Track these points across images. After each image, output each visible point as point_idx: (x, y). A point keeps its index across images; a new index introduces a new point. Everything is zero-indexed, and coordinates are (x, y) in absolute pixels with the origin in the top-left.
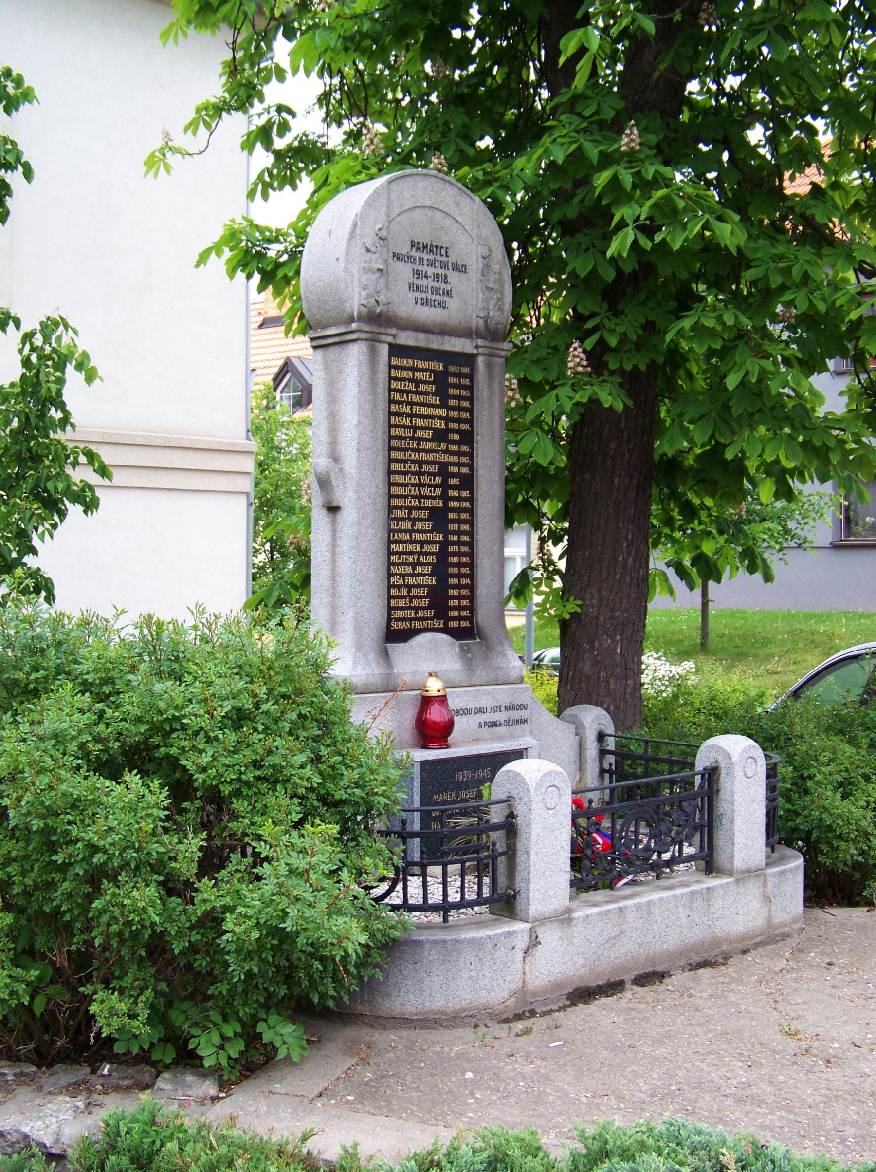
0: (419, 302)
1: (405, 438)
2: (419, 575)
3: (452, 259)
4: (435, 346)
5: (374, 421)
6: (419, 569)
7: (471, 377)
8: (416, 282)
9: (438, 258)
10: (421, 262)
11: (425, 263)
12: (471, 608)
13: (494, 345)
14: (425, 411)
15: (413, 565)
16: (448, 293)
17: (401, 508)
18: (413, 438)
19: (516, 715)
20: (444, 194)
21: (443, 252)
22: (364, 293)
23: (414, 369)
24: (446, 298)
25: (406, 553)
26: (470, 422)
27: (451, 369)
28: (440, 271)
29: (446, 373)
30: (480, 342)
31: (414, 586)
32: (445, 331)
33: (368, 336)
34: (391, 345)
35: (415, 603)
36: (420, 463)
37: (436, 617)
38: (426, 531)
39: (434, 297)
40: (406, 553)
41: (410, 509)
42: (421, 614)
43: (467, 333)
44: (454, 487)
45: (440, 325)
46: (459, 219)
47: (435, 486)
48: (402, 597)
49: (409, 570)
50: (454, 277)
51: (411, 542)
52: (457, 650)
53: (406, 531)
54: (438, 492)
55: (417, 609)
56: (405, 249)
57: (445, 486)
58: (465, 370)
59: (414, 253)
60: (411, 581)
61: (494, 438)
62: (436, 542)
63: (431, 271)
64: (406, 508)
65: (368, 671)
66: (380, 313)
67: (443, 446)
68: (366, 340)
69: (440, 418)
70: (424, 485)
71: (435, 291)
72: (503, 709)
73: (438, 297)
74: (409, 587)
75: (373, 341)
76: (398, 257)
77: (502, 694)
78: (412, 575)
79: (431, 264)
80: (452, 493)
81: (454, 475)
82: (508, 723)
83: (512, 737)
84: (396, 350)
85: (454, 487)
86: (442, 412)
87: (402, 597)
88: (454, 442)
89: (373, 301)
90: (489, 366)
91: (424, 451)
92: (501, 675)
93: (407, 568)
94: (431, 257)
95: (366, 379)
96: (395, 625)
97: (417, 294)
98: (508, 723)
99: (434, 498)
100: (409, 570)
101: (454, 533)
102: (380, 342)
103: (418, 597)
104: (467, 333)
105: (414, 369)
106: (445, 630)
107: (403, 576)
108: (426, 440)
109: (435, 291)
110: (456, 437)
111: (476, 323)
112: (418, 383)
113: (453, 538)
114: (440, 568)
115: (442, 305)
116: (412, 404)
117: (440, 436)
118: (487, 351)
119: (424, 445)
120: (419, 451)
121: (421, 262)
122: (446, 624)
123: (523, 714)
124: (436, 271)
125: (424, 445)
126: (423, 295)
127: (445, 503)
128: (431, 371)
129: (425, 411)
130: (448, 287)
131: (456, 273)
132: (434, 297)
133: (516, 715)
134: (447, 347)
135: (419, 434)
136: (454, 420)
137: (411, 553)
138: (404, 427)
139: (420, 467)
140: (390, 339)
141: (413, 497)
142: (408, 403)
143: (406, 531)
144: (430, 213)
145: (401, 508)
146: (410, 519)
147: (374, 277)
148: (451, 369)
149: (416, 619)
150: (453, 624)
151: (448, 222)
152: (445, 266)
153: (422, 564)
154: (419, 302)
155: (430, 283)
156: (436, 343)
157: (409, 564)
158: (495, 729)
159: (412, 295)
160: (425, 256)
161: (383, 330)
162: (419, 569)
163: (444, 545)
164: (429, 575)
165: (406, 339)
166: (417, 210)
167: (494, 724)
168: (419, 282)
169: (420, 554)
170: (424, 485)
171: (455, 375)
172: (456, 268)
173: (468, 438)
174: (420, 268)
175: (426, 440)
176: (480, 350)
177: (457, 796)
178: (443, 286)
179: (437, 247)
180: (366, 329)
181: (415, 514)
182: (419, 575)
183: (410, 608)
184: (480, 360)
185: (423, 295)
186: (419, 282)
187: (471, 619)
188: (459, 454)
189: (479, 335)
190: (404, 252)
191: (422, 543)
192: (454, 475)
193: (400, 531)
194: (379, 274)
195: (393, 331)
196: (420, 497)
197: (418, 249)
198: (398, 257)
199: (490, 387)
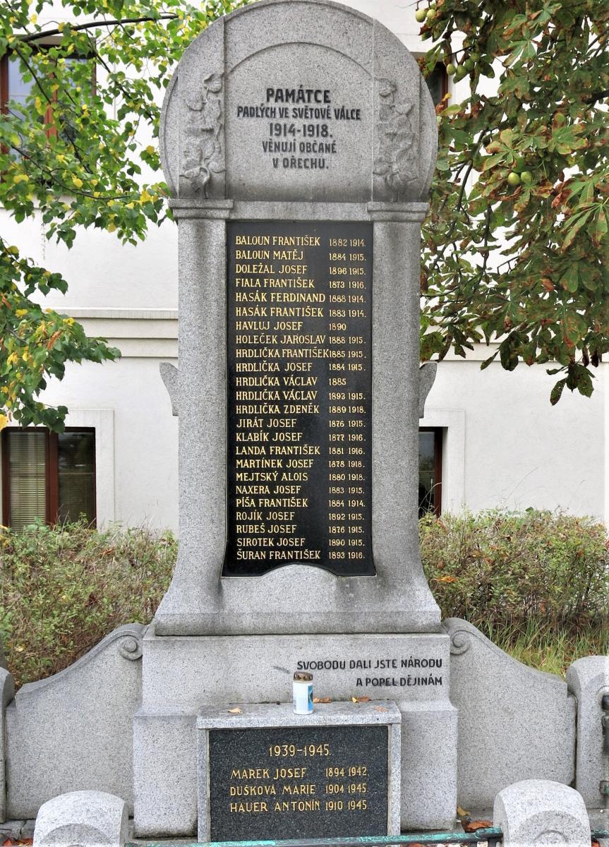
0: (280, 164)
1: (258, 333)
2: (280, 496)
3: (337, 102)
4: (300, 216)
5: (204, 315)
6: (279, 489)
7: (368, 251)
8: (275, 139)
9: (313, 105)
10: (284, 113)
11: (291, 114)
12: (367, 537)
13: (397, 206)
14: (287, 297)
15: (272, 485)
16: (330, 149)
17: (252, 417)
18: (271, 332)
19: (423, 672)
20: (321, 22)
21: (321, 97)
22: (184, 162)
23: (270, 248)
24: (325, 155)
25: (260, 470)
26: (368, 307)
27: (333, 242)
28: (315, 122)
29: (325, 249)
30: (371, 205)
31: (273, 509)
32: (323, 196)
33: (192, 213)
34: (229, 223)
35: (274, 529)
36: (283, 362)
37: (309, 545)
38: (291, 444)
39: (305, 156)
40: (260, 470)
41: (267, 417)
42: (283, 542)
43: (362, 195)
44: (338, 389)
45: (316, 189)
46: (347, 51)
47: (307, 389)
48: (253, 523)
49: (264, 490)
50: (338, 128)
51: (268, 457)
52: (334, 588)
53: (260, 444)
54: (311, 395)
55: (276, 537)
56: (258, 100)
57: (323, 388)
58: (356, 243)
59: (272, 103)
60: (267, 503)
61: (400, 326)
62: (308, 457)
63: (299, 123)
64: (259, 416)
65: (185, 609)
66: (210, 181)
67: (320, 339)
68: (190, 218)
69: (316, 304)
70: (289, 388)
71: (306, 147)
72: (398, 664)
73: (312, 155)
74: (265, 511)
75: (200, 220)
76: (246, 112)
77: (401, 647)
78: (271, 496)
79: (300, 114)
80: (333, 396)
81: (337, 374)
82: (405, 682)
83: (413, 699)
84: (233, 227)
85: (338, 389)
86: (319, 298)
87: (253, 523)
88: (337, 333)
89: (197, 169)
90: (394, 236)
91: (289, 346)
92: (401, 622)
93: (262, 488)
94: (301, 105)
95: (190, 264)
96: (241, 555)
97: (278, 155)
98: (405, 682)
99: (306, 403)
100: (264, 490)
101: (336, 444)
102: (212, 218)
103: (279, 523)
104: (362, 195)
105: (270, 248)
106: (323, 563)
107: (256, 497)
108: (292, 333)
109: (306, 147)
110: (341, 327)
111: (375, 182)
112: (279, 264)
113: (333, 451)
114: (315, 486)
115: (321, 164)
116: (268, 290)
117: (309, 327)
118: (389, 215)
119: (288, 339)
120: (280, 347)
121: (284, 113)
122: (324, 555)
123: (435, 672)
124: (307, 122)
125: (288, 339)
126: (288, 155)
127: (324, 409)
128: (299, 248)
129: (287, 297)
130: (330, 141)
131: (340, 122)
132: (305, 156)
133: (423, 672)
134: (322, 216)
135: (280, 326)
136: (337, 306)
137: (269, 470)
138: (257, 319)
139: (283, 366)
140: (225, 214)
141: (271, 402)
142: (262, 290)
143: (260, 444)
144: (300, 51)
145: (252, 417)
146: (265, 430)
147: (197, 141)
148: (333, 242)
149: (275, 548)
150: (333, 555)
151: (330, 58)
152: (324, 114)
153: (285, 483)
154: (280, 164)
155: (299, 138)
156: (303, 212)
157: (264, 483)
158: (384, 687)
159: (268, 157)
160: (290, 105)
161: (209, 204)
162: (279, 489)
163: (324, 458)
164: (296, 496)
165: (250, 211)
166: (278, 50)
167: (385, 682)
168: (282, 139)
169: (280, 471)
170: (289, 388)
171: (339, 250)
172: (341, 114)
173: (364, 328)
174: (282, 122)
175: (292, 333)
176: (375, 216)
177: (272, 774)
178: (320, 140)
179: (309, 92)
180: (184, 205)
181: (273, 423)
182: (280, 496)
183: (267, 535)
184: (379, 230)
185: (288, 155)
186: (282, 139)
187: (368, 548)
188: (346, 347)
189: (378, 197)
190: (257, 103)
191: (285, 458)
192: (337, 374)
193: (251, 444)
194: (206, 136)
195: (229, 203)
196: (281, 403)
197: (279, 98)
198: (246, 112)
199: (395, 260)
